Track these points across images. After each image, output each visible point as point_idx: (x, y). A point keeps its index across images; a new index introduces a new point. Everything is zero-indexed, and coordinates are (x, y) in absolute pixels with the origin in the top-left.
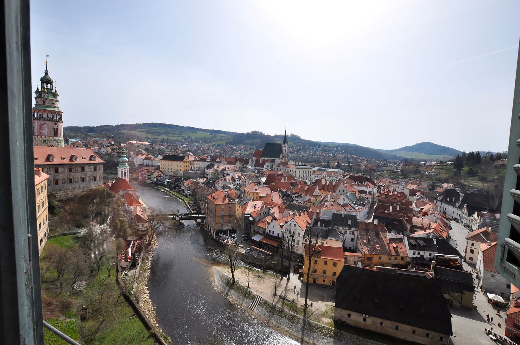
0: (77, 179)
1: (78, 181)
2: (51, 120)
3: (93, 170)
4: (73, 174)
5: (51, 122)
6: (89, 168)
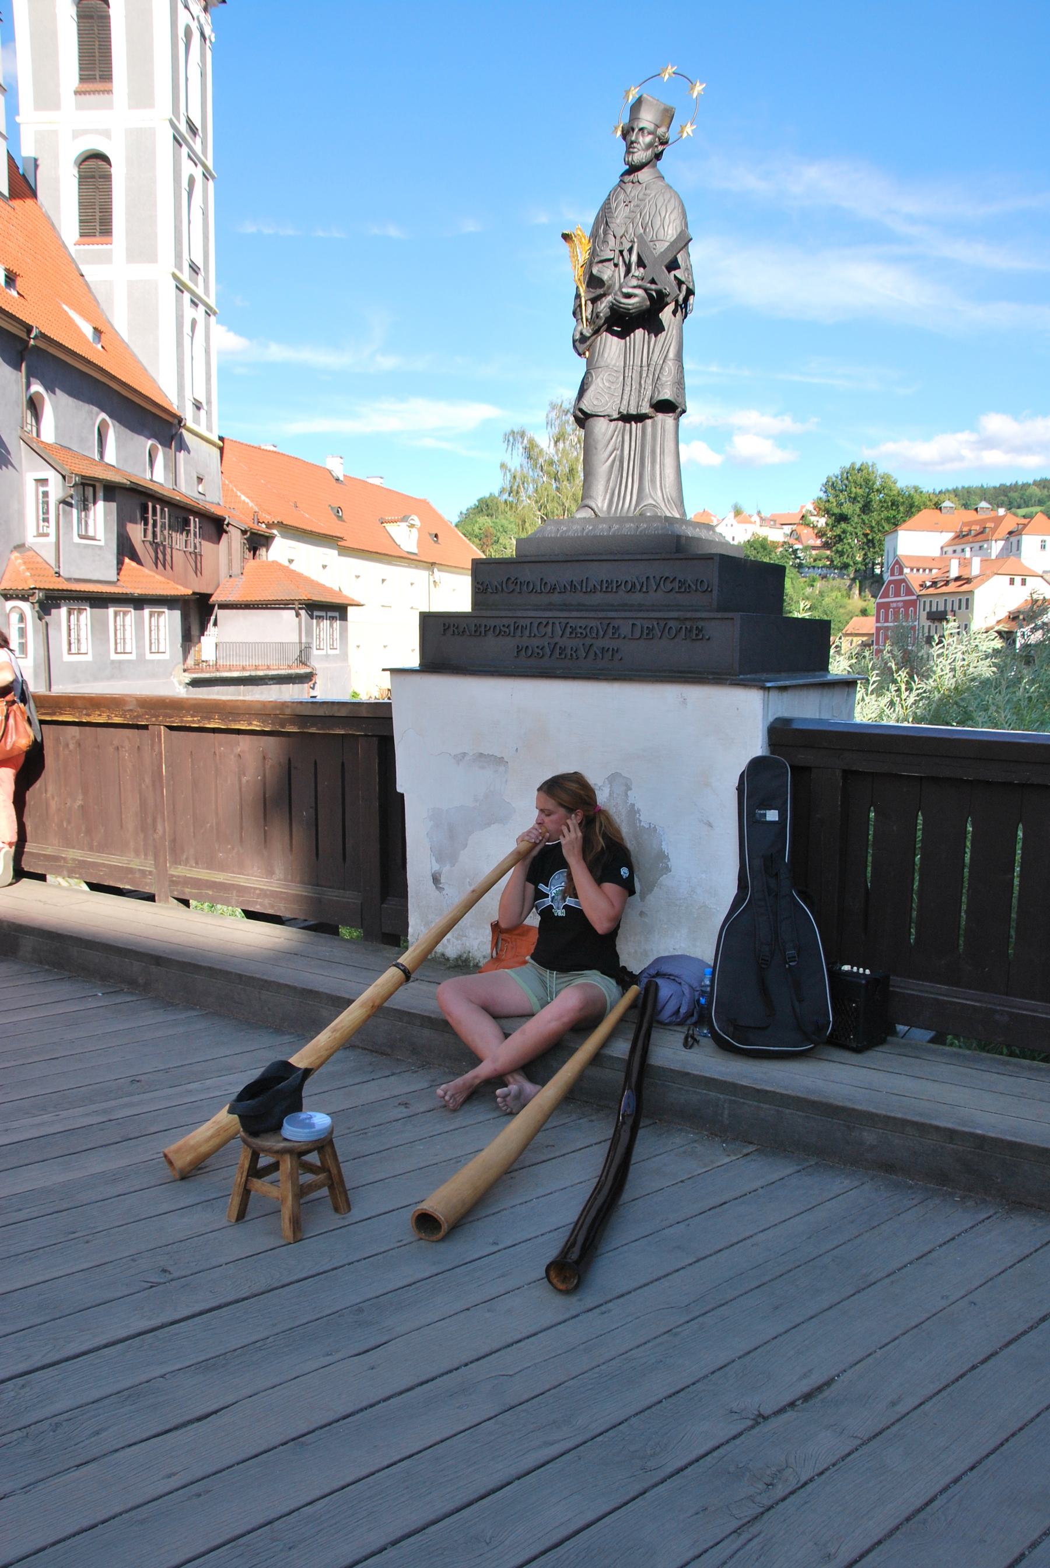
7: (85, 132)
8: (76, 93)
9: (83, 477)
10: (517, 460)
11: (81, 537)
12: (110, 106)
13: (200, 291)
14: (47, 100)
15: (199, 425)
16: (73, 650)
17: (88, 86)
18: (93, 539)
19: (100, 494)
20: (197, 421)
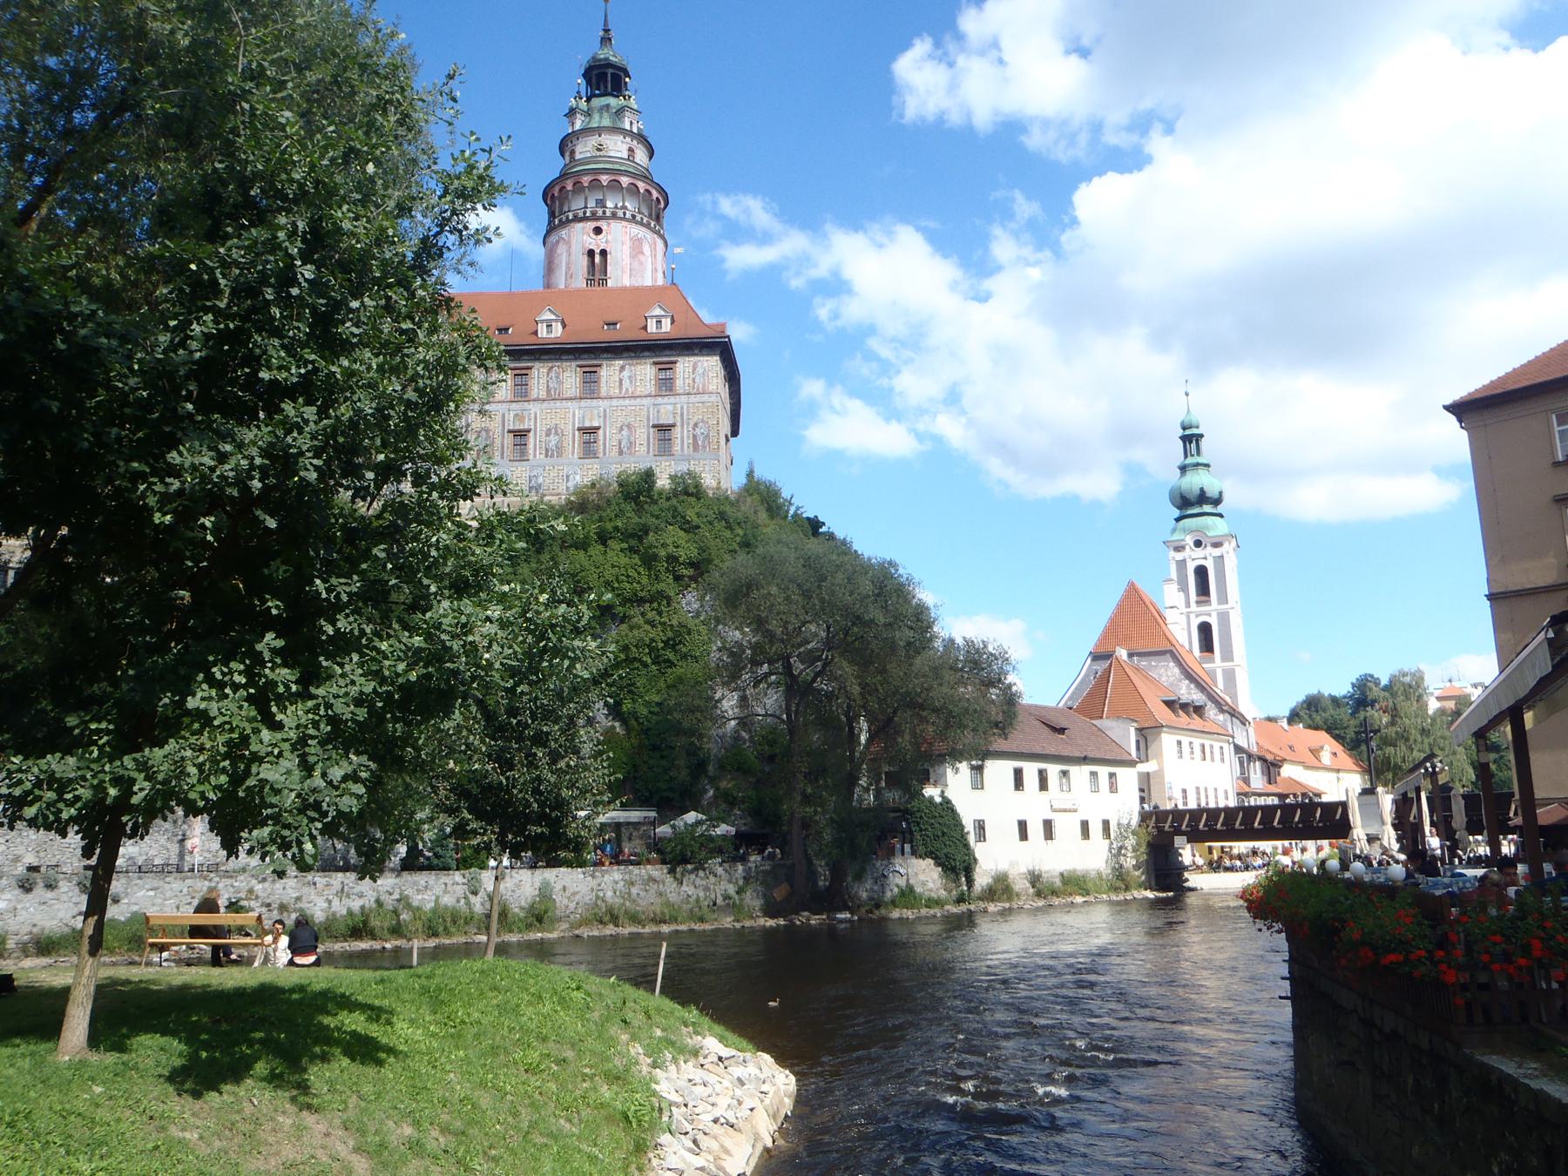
0: (553, 440)
1: (559, 450)
2: (581, 215)
3: (650, 387)
4: (534, 408)
5: (580, 225)
6: (626, 374)
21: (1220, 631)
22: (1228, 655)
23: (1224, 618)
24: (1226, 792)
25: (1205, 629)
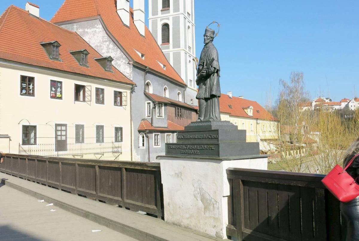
7: (163, 19)
8: (162, 11)
9: (159, 102)
10: (282, 88)
11: (158, 116)
12: (169, 13)
13: (191, 53)
14: (155, 13)
15: (191, 86)
16: (156, 145)
17: (164, 9)
18: (162, 117)
19: (163, 105)
20: (191, 85)
21: (173, 29)
22: (177, 45)
23: (176, 20)
24: (119, 130)
25: (166, 27)
